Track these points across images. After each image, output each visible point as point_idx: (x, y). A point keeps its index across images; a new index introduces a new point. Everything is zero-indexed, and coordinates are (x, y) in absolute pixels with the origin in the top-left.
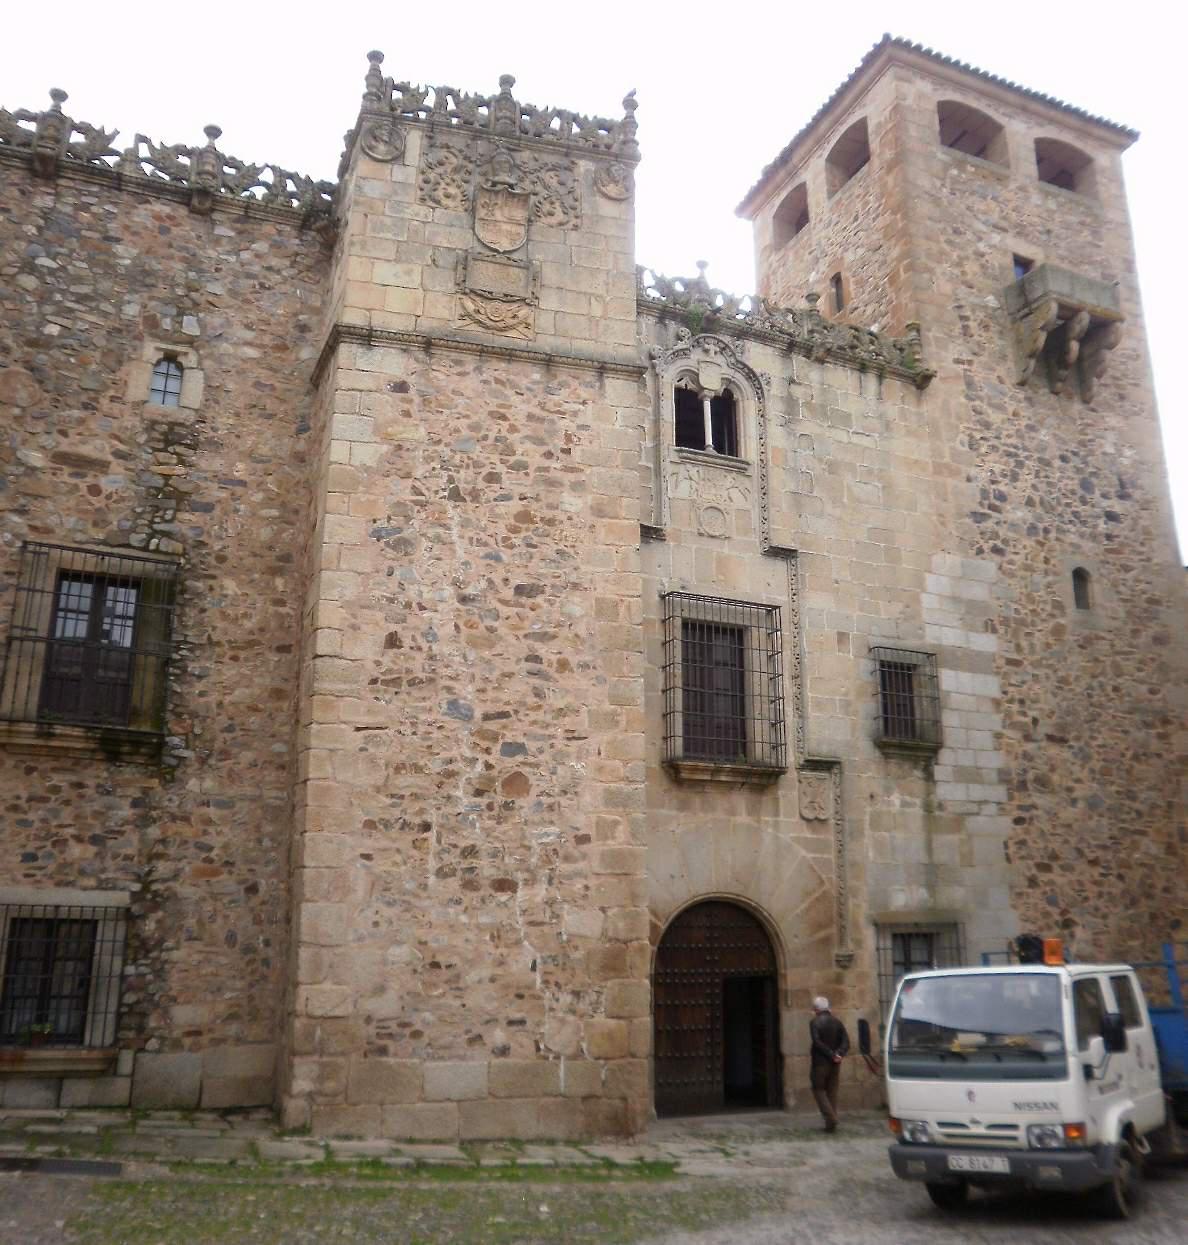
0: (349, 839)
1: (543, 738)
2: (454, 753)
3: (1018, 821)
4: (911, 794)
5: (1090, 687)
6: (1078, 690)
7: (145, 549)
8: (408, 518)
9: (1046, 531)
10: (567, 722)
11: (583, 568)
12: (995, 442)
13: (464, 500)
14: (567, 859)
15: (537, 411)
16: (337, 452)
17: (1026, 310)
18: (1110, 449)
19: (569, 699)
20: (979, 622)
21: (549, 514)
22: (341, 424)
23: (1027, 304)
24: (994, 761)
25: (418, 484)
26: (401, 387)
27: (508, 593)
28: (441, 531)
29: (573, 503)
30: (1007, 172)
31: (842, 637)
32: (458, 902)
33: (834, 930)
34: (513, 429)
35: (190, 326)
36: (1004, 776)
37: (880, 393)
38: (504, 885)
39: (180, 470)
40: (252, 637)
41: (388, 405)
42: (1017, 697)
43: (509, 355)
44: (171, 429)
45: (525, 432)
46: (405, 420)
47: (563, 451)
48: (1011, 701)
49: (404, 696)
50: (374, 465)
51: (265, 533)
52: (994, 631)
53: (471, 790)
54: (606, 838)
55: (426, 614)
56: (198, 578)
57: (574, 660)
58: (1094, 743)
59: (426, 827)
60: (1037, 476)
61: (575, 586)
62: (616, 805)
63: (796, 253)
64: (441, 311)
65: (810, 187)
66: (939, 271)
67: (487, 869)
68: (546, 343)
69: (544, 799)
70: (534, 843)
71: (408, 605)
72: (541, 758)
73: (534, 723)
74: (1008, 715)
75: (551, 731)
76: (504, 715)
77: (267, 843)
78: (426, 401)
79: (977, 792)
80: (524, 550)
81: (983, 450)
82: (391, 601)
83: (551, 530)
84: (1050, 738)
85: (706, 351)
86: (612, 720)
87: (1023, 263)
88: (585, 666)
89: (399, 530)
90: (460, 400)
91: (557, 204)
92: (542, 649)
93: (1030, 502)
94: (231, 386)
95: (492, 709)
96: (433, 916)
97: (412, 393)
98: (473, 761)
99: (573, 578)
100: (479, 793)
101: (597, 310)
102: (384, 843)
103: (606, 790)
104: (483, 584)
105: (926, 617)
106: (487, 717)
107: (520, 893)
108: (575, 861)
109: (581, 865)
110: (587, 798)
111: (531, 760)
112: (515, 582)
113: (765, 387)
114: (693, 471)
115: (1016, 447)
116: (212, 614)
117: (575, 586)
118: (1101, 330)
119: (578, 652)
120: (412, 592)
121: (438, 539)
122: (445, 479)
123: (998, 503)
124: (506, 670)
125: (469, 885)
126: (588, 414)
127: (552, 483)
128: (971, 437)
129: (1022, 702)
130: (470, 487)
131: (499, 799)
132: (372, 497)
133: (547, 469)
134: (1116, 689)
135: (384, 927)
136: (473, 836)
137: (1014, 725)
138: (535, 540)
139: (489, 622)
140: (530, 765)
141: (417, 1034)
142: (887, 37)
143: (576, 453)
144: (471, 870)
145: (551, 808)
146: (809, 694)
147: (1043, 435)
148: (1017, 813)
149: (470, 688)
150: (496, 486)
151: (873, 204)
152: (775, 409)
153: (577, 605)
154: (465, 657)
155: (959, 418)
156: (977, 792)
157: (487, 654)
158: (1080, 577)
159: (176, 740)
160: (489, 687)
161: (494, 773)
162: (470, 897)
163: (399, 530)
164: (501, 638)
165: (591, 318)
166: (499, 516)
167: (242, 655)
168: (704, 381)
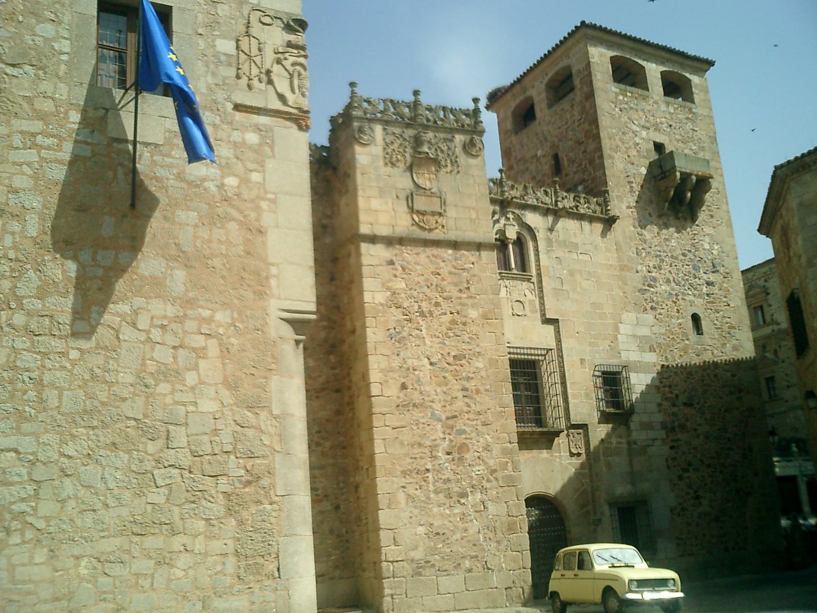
3: (672, 448)
4: (620, 437)
5: (703, 376)
6: (697, 378)
8: (403, 327)
9: (677, 295)
12: (648, 250)
13: (426, 317)
15: (454, 270)
16: (367, 297)
17: (663, 175)
18: (707, 246)
20: (647, 347)
21: (464, 320)
22: (368, 284)
23: (663, 172)
24: (658, 418)
26: (391, 263)
27: (451, 360)
28: (418, 332)
29: (473, 314)
30: (645, 93)
31: (582, 361)
33: (590, 507)
34: (443, 279)
36: (664, 426)
37: (591, 230)
40: (325, 386)
41: (386, 272)
42: (668, 384)
43: (437, 243)
45: (449, 280)
46: (395, 279)
47: (466, 288)
48: (664, 387)
50: (384, 303)
51: (323, 335)
52: (655, 351)
55: (416, 373)
57: (482, 389)
58: (707, 405)
60: (671, 266)
63: (528, 137)
64: (403, 224)
65: (536, 100)
66: (616, 157)
68: (452, 236)
71: (408, 369)
74: (664, 394)
76: (455, 417)
77: (341, 485)
78: (404, 269)
79: (651, 434)
81: (644, 255)
82: (401, 367)
84: (685, 404)
85: (508, 219)
87: (659, 147)
90: (418, 267)
91: (449, 161)
92: (467, 385)
93: (668, 281)
97: (396, 264)
99: (478, 350)
101: (474, 215)
105: (621, 346)
106: (448, 418)
107: (470, 498)
111: (468, 436)
112: (453, 354)
113: (537, 234)
114: (507, 282)
115: (660, 251)
118: (702, 184)
120: (410, 362)
122: (417, 307)
123: (652, 283)
126: (476, 269)
127: (463, 305)
128: (637, 249)
129: (670, 386)
131: (457, 456)
132: (386, 318)
133: (460, 298)
134: (715, 376)
137: (666, 399)
140: (469, 439)
141: (433, 566)
142: (583, 23)
143: (472, 289)
146: (569, 391)
147: (673, 243)
148: (671, 444)
150: (439, 308)
151: (577, 117)
152: (542, 245)
154: (436, 391)
155: (631, 239)
156: (651, 434)
158: (696, 319)
165: (471, 220)
167: (320, 395)
168: (508, 235)
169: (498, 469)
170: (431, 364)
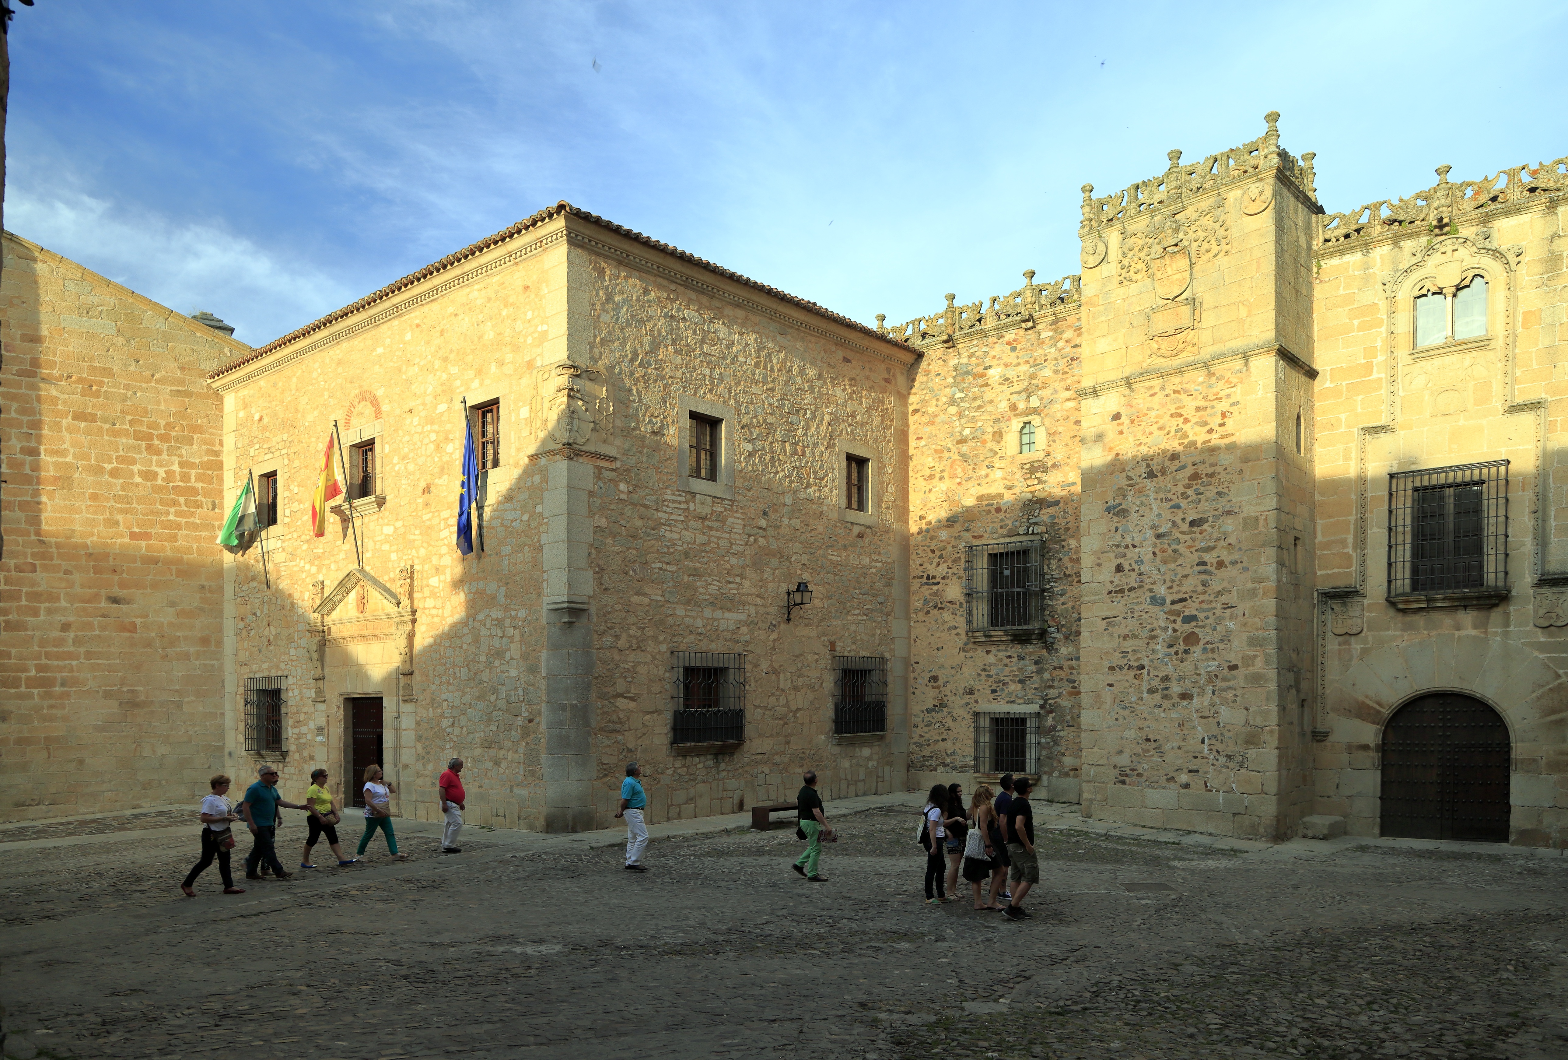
0: (1101, 676)
1: (1208, 610)
2: (1155, 625)
7: (1027, 534)
10: (1224, 598)
11: (1234, 500)
14: (1224, 679)
19: (1225, 584)
21: (1210, 470)
25: (1129, 474)
26: (1117, 417)
27: (1185, 527)
28: (1144, 498)
32: (1160, 706)
35: (1035, 402)
38: (1185, 696)
39: (1039, 487)
44: (1032, 465)
49: (1126, 598)
53: (1166, 645)
54: (1249, 666)
56: (1056, 543)
57: (1227, 559)
59: (1142, 667)
61: (1229, 513)
62: (1255, 646)
67: (1176, 689)
69: (1209, 646)
70: (1202, 672)
72: (1208, 621)
73: (1202, 602)
75: (1214, 604)
76: (1185, 600)
78: (1132, 422)
80: (1195, 497)
83: (1213, 480)
86: (1253, 593)
88: (1234, 563)
89: (1120, 504)
94: (1060, 429)
95: (1176, 597)
96: (1145, 715)
97: (1124, 419)
98: (1166, 629)
100: (1170, 646)
102: (1119, 678)
103: (1249, 637)
104: (1170, 524)
106: (1173, 603)
108: (1229, 680)
109: (1232, 683)
110: (1236, 643)
111: (1200, 624)
112: (1190, 518)
116: (1066, 559)
117: (1229, 513)
119: (1230, 554)
121: (1142, 504)
124: (1184, 573)
125: (1165, 697)
130: (1159, 468)
131: (1182, 647)
135: (1121, 720)
136: (1168, 670)
138: (1202, 489)
139: (1174, 547)
140: (1200, 627)
144: (1167, 689)
145: (1213, 650)
149: (1163, 587)
150: (1176, 462)
153: (1229, 525)
157: (1173, 566)
159: (1052, 629)
160: (1175, 585)
161: (1178, 633)
162: (1166, 704)
163: (1120, 504)
164: (1181, 555)
166: (1179, 480)
169: (1240, 664)
170: (1158, 536)
